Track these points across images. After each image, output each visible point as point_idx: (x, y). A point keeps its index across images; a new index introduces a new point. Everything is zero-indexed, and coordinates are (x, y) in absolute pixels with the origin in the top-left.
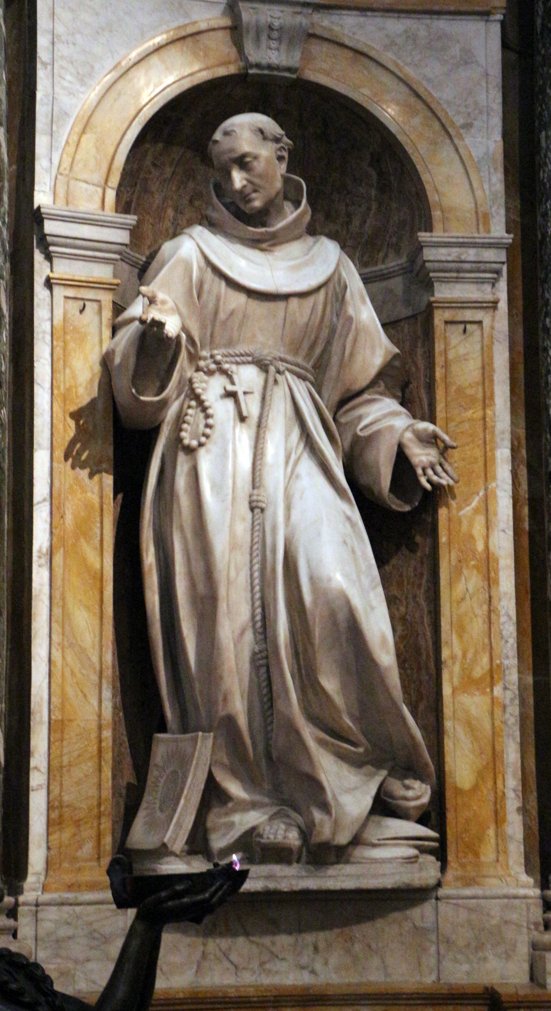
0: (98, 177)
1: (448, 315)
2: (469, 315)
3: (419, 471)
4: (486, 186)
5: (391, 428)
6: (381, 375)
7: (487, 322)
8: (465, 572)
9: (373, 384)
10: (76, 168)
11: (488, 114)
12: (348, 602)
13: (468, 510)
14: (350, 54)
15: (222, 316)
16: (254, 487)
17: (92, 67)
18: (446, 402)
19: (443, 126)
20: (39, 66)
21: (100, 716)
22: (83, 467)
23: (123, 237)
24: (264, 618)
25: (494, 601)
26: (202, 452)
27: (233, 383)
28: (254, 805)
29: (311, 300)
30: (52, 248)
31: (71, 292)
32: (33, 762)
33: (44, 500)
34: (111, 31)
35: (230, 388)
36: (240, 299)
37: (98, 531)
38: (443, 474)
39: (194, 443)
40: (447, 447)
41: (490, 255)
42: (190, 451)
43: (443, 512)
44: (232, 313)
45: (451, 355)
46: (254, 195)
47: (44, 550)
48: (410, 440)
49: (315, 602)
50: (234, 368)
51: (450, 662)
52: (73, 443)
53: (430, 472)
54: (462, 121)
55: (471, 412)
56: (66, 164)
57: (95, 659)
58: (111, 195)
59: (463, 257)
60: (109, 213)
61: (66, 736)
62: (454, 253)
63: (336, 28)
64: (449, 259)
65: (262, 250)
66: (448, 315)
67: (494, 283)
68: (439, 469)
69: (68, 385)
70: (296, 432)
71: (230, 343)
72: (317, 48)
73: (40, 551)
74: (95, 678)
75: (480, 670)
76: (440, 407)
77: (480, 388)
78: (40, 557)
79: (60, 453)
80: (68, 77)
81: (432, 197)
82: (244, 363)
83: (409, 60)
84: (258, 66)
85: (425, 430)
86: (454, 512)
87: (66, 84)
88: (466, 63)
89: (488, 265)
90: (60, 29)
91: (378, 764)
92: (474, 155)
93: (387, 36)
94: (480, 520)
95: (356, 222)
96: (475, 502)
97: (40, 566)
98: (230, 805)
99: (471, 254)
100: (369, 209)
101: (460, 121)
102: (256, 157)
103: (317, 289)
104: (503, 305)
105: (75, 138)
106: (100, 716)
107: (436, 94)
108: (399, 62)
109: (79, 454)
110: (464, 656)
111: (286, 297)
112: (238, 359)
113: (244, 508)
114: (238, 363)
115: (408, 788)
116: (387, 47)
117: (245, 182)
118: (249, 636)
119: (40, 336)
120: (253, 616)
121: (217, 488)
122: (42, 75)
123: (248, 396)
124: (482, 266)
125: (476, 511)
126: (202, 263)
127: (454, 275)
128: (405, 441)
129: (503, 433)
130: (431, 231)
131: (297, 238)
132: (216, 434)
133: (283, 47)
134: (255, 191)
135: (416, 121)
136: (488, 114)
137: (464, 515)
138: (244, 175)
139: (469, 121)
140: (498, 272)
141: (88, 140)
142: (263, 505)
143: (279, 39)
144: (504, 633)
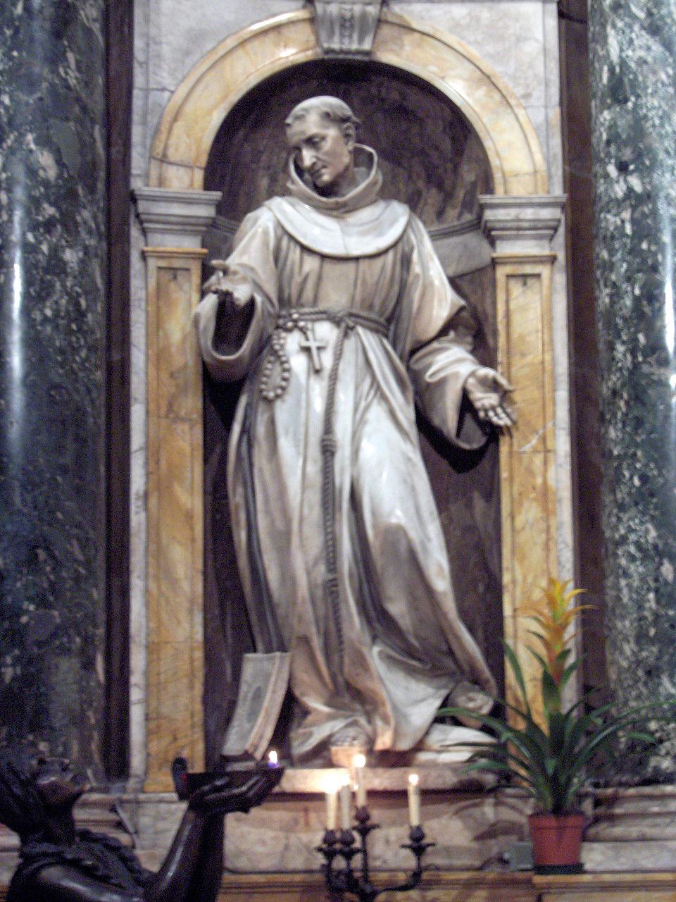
2: (528, 269)
5: (456, 375)
9: (443, 332)
13: (527, 448)
19: (504, 97)
20: (136, 65)
23: (207, 212)
25: (553, 530)
26: (278, 403)
27: (307, 339)
28: (330, 717)
29: (379, 262)
35: (305, 344)
38: (503, 415)
39: (271, 395)
46: (324, 171)
47: (141, 493)
49: (376, 536)
50: (309, 325)
51: (510, 587)
59: (522, 216)
61: (163, 656)
64: (508, 218)
65: (336, 217)
66: (508, 269)
67: (551, 238)
68: (499, 410)
69: (161, 345)
83: (472, 39)
99: (529, 214)
102: (323, 138)
104: (561, 256)
110: (525, 580)
111: (357, 259)
115: (471, 700)
116: (451, 31)
117: (314, 160)
119: (136, 303)
126: (280, 232)
128: (470, 387)
131: (373, 202)
134: (324, 167)
139: (529, 91)
140: (555, 229)
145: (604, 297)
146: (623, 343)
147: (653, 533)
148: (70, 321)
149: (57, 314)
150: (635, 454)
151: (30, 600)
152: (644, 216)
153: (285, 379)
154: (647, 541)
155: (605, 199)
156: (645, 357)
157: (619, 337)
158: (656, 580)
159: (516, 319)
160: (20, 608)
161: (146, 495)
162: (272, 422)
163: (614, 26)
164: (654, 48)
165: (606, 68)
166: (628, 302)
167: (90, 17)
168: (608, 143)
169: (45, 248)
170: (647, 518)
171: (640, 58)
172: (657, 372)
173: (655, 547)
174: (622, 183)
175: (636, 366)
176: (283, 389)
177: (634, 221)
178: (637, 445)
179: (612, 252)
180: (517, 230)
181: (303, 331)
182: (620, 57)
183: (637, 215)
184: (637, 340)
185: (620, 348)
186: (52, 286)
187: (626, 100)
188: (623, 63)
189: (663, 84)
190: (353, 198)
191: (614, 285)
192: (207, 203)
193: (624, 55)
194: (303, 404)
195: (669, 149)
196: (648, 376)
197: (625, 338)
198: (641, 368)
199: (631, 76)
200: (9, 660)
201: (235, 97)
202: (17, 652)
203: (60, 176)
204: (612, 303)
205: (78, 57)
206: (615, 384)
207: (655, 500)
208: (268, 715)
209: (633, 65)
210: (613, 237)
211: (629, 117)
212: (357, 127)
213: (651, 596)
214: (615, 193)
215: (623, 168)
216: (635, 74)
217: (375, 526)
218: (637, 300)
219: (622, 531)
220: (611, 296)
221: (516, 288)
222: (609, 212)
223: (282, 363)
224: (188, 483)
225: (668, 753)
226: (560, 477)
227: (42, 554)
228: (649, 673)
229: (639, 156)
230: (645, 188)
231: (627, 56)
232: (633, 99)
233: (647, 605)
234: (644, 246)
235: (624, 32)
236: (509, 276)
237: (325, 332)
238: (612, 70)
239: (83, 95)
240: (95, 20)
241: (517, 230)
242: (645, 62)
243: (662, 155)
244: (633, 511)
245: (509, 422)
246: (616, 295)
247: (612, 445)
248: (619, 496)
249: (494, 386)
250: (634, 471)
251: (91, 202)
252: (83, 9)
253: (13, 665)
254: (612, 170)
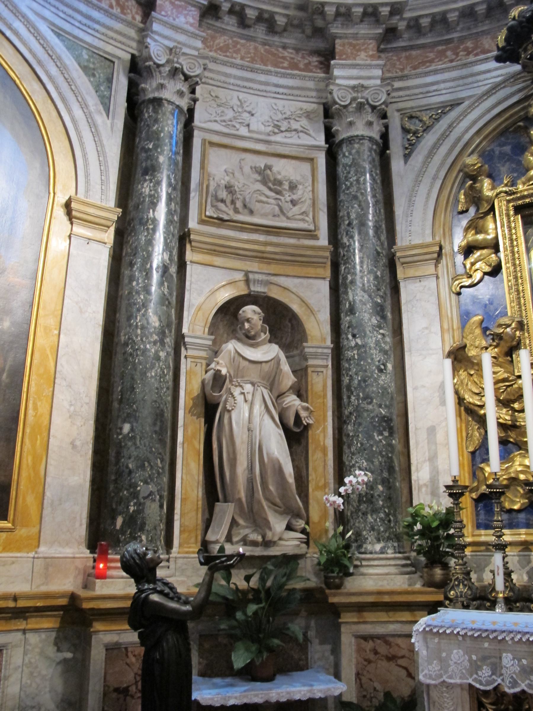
0: (203, 324)
2: (319, 369)
5: (294, 405)
6: (291, 388)
7: (325, 372)
12: (279, 461)
13: (318, 432)
14: (282, 289)
15: (241, 368)
16: (249, 423)
19: (311, 311)
21: (198, 497)
22: (194, 415)
23: (210, 343)
24: (251, 466)
26: (233, 412)
28: (247, 527)
31: (193, 360)
32: (176, 512)
36: (246, 363)
40: (312, 411)
41: (326, 351)
42: (229, 411)
43: (310, 432)
44: (244, 367)
45: (314, 382)
50: (244, 385)
52: (191, 408)
56: (193, 320)
57: (196, 478)
58: (207, 330)
60: (206, 335)
66: (312, 369)
70: (263, 407)
71: (243, 377)
72: (272, 287)
74: (196, 484)
75: (322, 483)
76: (310, 398)
79: (187, 411)
81: (308, 332)
84: (254, 291)
90: (193, 280)
91: (287, 514)
94: (322, 435)
95: (284, 339)
96: (321, 429)
99: (320, 350)
101: (316, 309)
102: (253, 319)
104: (330, 366)
106: (198, 497)
111: (261, 363)
113: (246, 430)
118: (247, 472)
120: (248, 466)
121: (237, 423)
125: (321, 432)
131: (265, 344)
135: (303, 309)
141: (200, 314)
143: (261, 284)
145: (346, 380)
147: (365, 464)
148: (160, 378)
149: (156, 375)
151: (142, 481)
160: (137, 484)
162: (230, 419)
166: (356, 382)
168: (349, 327)
169: (153, 350)
175: (359, 404)
177: (358, 354)
179: (350, 365)
180: (316, 356)
181: (241, 386)
183: (359, 352)
185: (353, 398)
186: (155, 364)
187: (355, 314)
188: (354, 301)
191: (351, 376)
192: (209, 340)
197: (355, 394)
200: (132, 504)
202: (135, 501)
203: (160, 325)
204: (350, 382)
208: (226, 525)
210: (350, 359)
215: (354, 336)
218: (359, 381)
219: (353, 462)
220: (350, 380)
221: (315, 375)
226: (329, 442)
227: (146, 464)
228: (363, 514)
234: (362, 363)
236: (313, 372)
237: (248, 388)
238: (350, 303)
241: (316, 356)
244: (358, 455)
246: (351, 379)
248: (352, 450)
249: (307, 409)
251: (170, 336)
253: (134, 506)
254: (350, 337)
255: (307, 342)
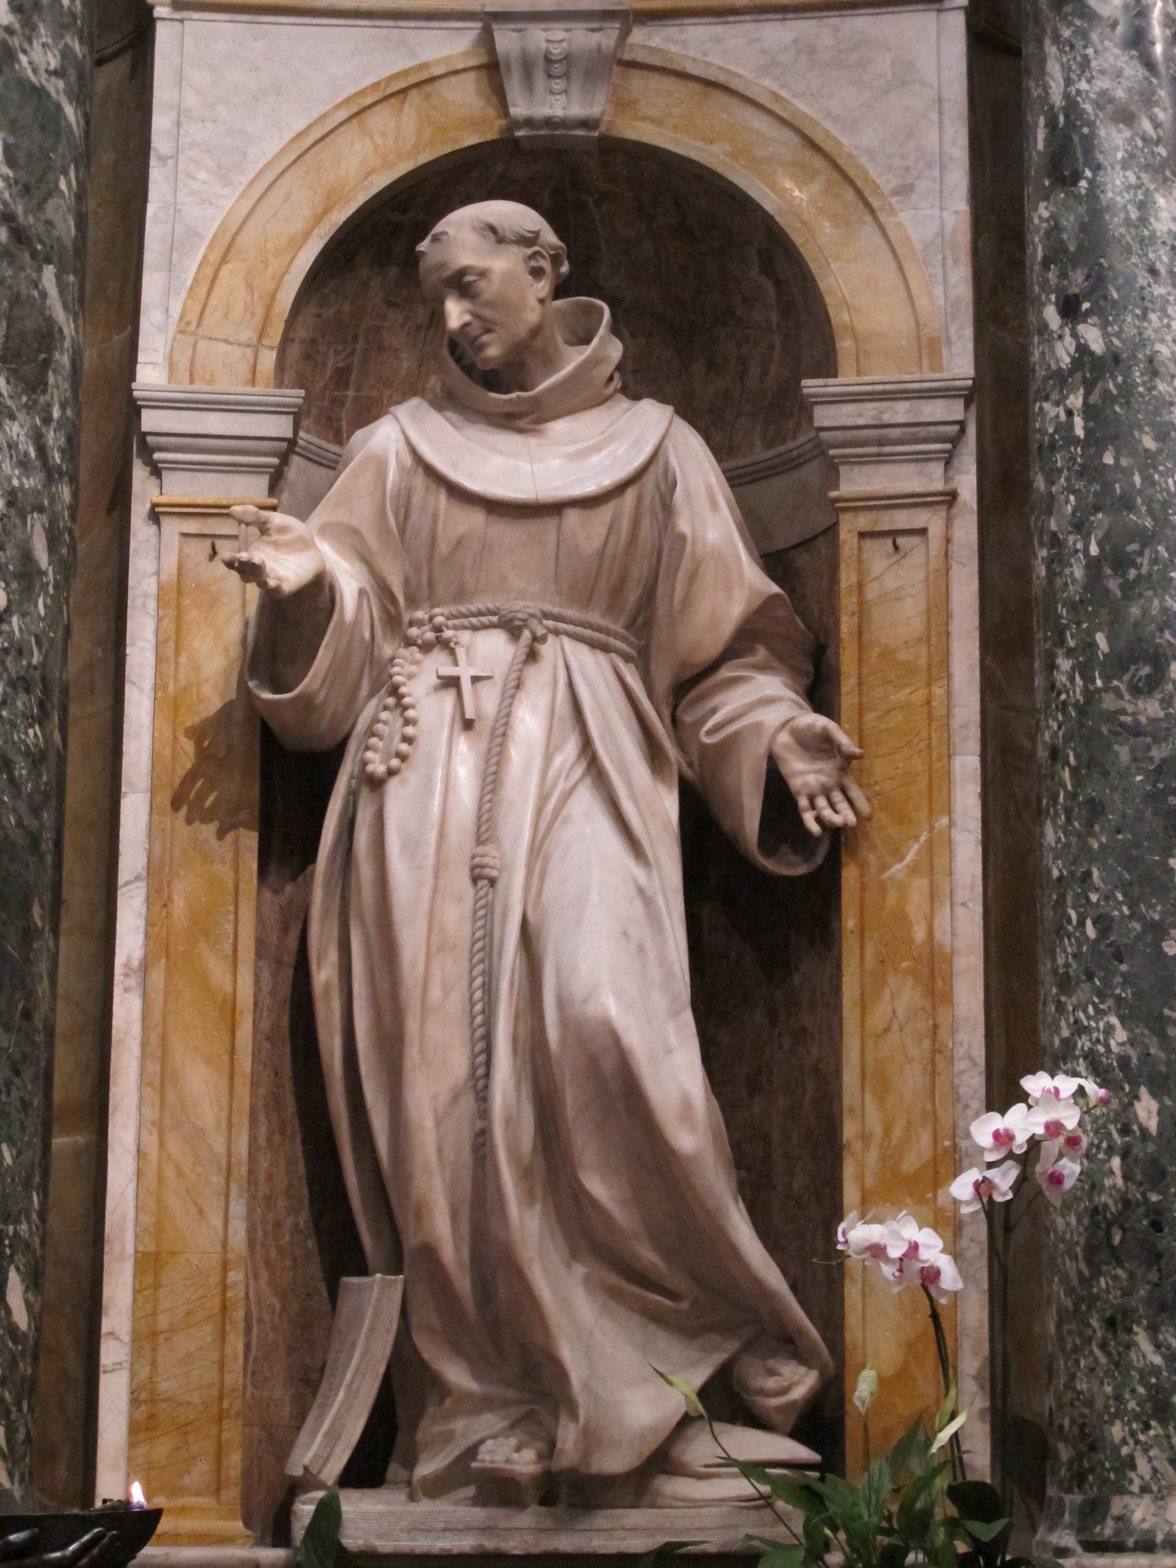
0: (247, 334)
1: (863, 521)
2: (902, 519)
3: (803, 802)
4: (938, 291)
5: (758, 727)
8: (892, 981)
9: (735, 649)
10: (207, 320)
11: (943, 167)
14: (697, 87)
15: (443, 548)
16: (479, 841)
17: (245, 155)
18: (860, 677)
19: (859, 193)
20: (153, 162)
21: (225, 1244)
22: (206, 818)
25: (943, 1033)
26: (393, 786)
27: (456, 663)
28: (488, 1404)
29: (606, 513)
30: (157, 456)
31: (192, 526)
32: (106, 1325)
33: (137, 878)
34: (279, 94)
35: (449, 670)
36: (476, 518)
37: (230, 928)
38: (843, 806)
41: (935, 410)
44: (459, 543)
45: (871, 592)
47: (135, 964)
48: (787, 747)
49: (563, 1038)
50: (465, 636)
51: (858, 1146)
52: (191, 777)
53: (821, 802)
54: (895, 183)
55: (908, 690)
56: (193, 317)
57: (219, 1146)
58: (268, 359)
59: (886, 418)
60: (263, 391)
61: (165, 1280)
62: (867, 413)
63: (674, 49)
64: (861, 421)
65: (521, 431)
66: (863, 521)
67: (948, 461)
68: (837, 796)
69: (182, 682)
71: (461, 594)
72: (638, 83)
73: (127, 965)
74: (217, 1180)
76: (848, 684)
77: (924, 650)
78: (126, 975)
79: (165, 798)
80: (202, 175)
81: (839, 317)
82: (485, 627)
84: (528, 122)
85: (810, 727)
86: (873, 871)
87: (197, 186)
88: (904, 83)
89: (932, 429)
90: (191, 99)
91: (727, 1329)
92: (914, 237)
93: (764, 51)
95: (754, 370)
97: (126, 990)
98: (448, 1402)
99: (900, 412)
100: (771, 347)
101: (887, 182)
102: (483, 274)
103: (619, 489)
105: (209, 271)
106: (225, 1244)
107: (847, 141)
108: (783, 93)
109: (201, 797)
110: (887, 1132)
111: (556, 508)
112: (474, 620)
113: (459, 879)
114: (475, 628)
115: (772, 1373)
116: (763, 70)
117: (467, 318)
119: (139, 602)
122: (157, 175)
123: (481, 685)
124: (922, 432)
125: (914, 870)
126: (408, 460)
127: (874, 450)
128: (777, 749)
129: (965, 726)
130: (835, 375)
132: (418, 754)
133: (575, 87)
134: (488, 331)
136: (943, 167)
137: (890, 878)
138: (466, 305)
139: (909, 180)
140: (956, 441)
141: (232, 275)
142: (494, 873)
143: (566, 75)
144: (962, 1090)
146: (1070, 653)
147: (1121, 1035)
150: (1088, 874)
152: (1107, 396)
153: (408, 740)
154: (1108, 1049)
155: (1041, 373)
156: (1107, 679)
157: (1062, 642)
158: (1125, 1130)
159: (878, 616)
161: (146, 967)
163: (1057, 39)
164: (1128, 71)
165: (1042, 121)
166: (1078, 571)
167: (42, 67)
170: (1110, 1002)
171: (1103, 93)
172: (1130, 708)
173: (1124, 1061)
174: (1068, 339)
175: (1091, 695)
176: (403, 757)
177: (1089, 411)
178: (1092, 857)
182: (1067, 96)
183: (1093, 399)
184: (1093, 645)
185: (1065, 664)
187: (1076, 176)
188: (1071, 105)
189: (1145, 139)
190: (550, 390)
192: (277, 410)
193: (1073, 90)
194: (439, 788)
195: (1159, 266)
196: (1112, 717)
197: (1071, 643)
198: (1100, 700)
199: (1085, 130)
201: (341, 215)
204: (1052, 574)
205: (11, 140)
206: (1055, 735)
207: (1124, 967)
208: (351, 1394)
209: (1088, 107)
210: (1053, 447)
211: (1082, 210)
212: (556, 260)
213: (1116, 1162)
214: (1057, 361)
215: (1070, 310)
216: (1091, 125)
217: (565, 1021)
218: (1094, 566)
219: (1066, 1033)
220: (1049, 562)
221: (878, 555)
222: (1047, 398)
223: (405, 708)
224: (228, 946)
225: (1145, 1489)
228: (1111, 1323)
229: (1098, 281)
230: (1108, 344)
231: (1079, 92)
232: (1088, 173)
233: (1108, 1182)
234: (1108, 459)
235: (1072, 47)
238: (1052, 124)
239: (19, 210)
240: (55, 73)
242: (1111, 100)
243: (1143, 279)
244: (1083, 992)
245: (851, 818)
247: (1048, 859)
248: (1060, 961)
249: (821, 746)
250: (1083, 903)
251: (29, 408)
252: (25, 52)
254: (1051, 315)
255: (827, 366)
